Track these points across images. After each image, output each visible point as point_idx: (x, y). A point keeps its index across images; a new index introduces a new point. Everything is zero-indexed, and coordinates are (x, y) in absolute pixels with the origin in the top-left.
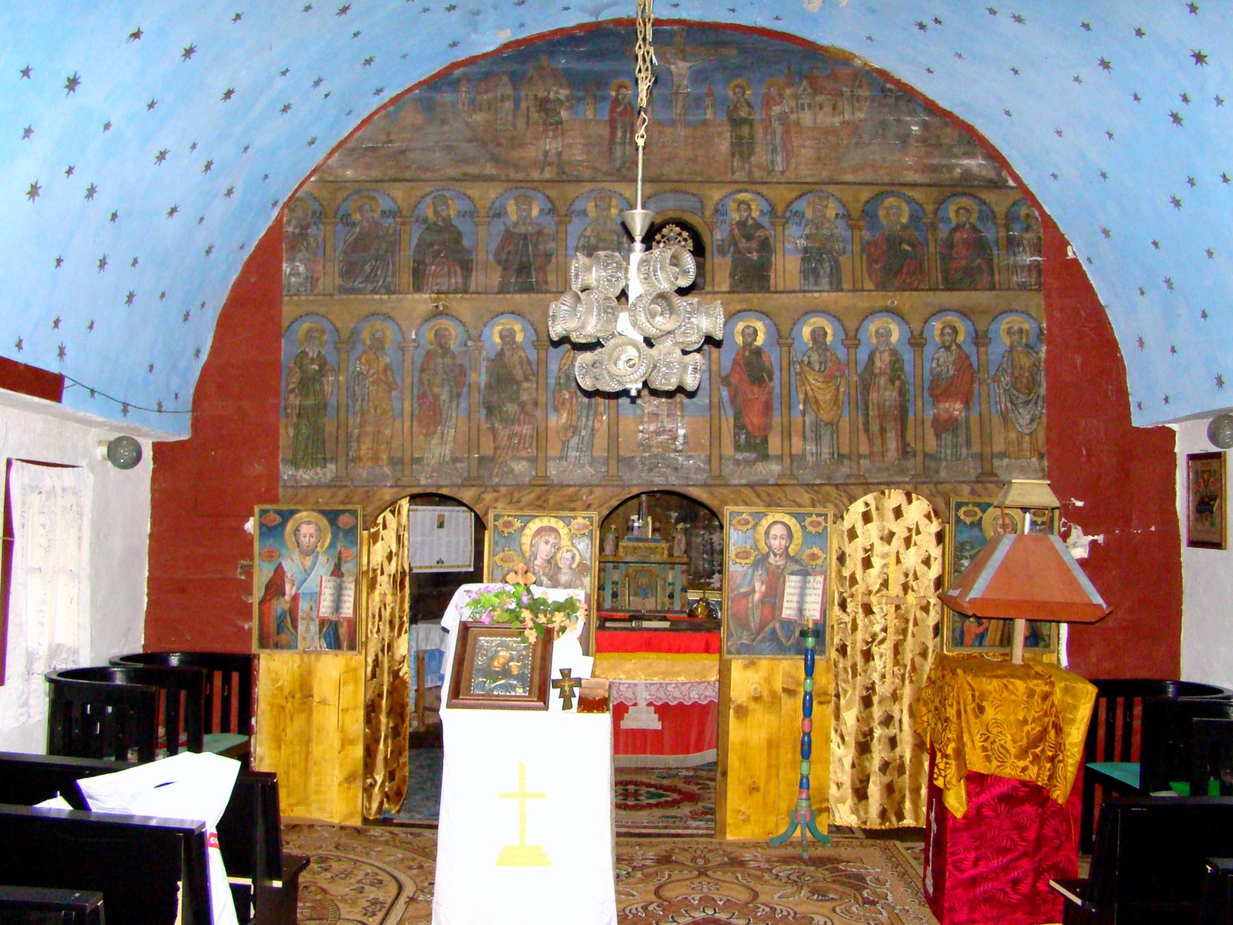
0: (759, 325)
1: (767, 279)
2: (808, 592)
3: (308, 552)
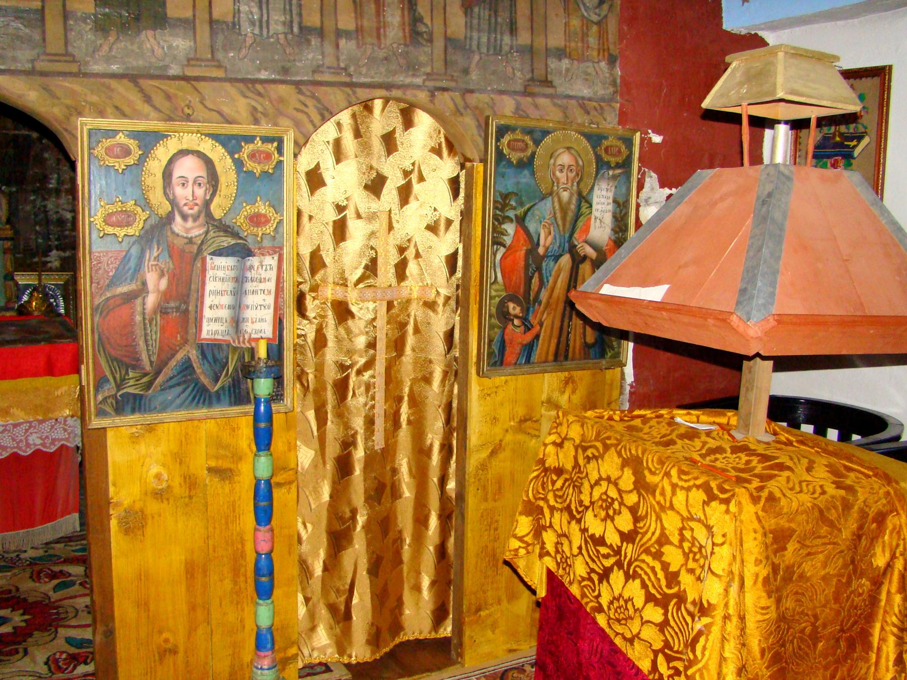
2: (249, 286)
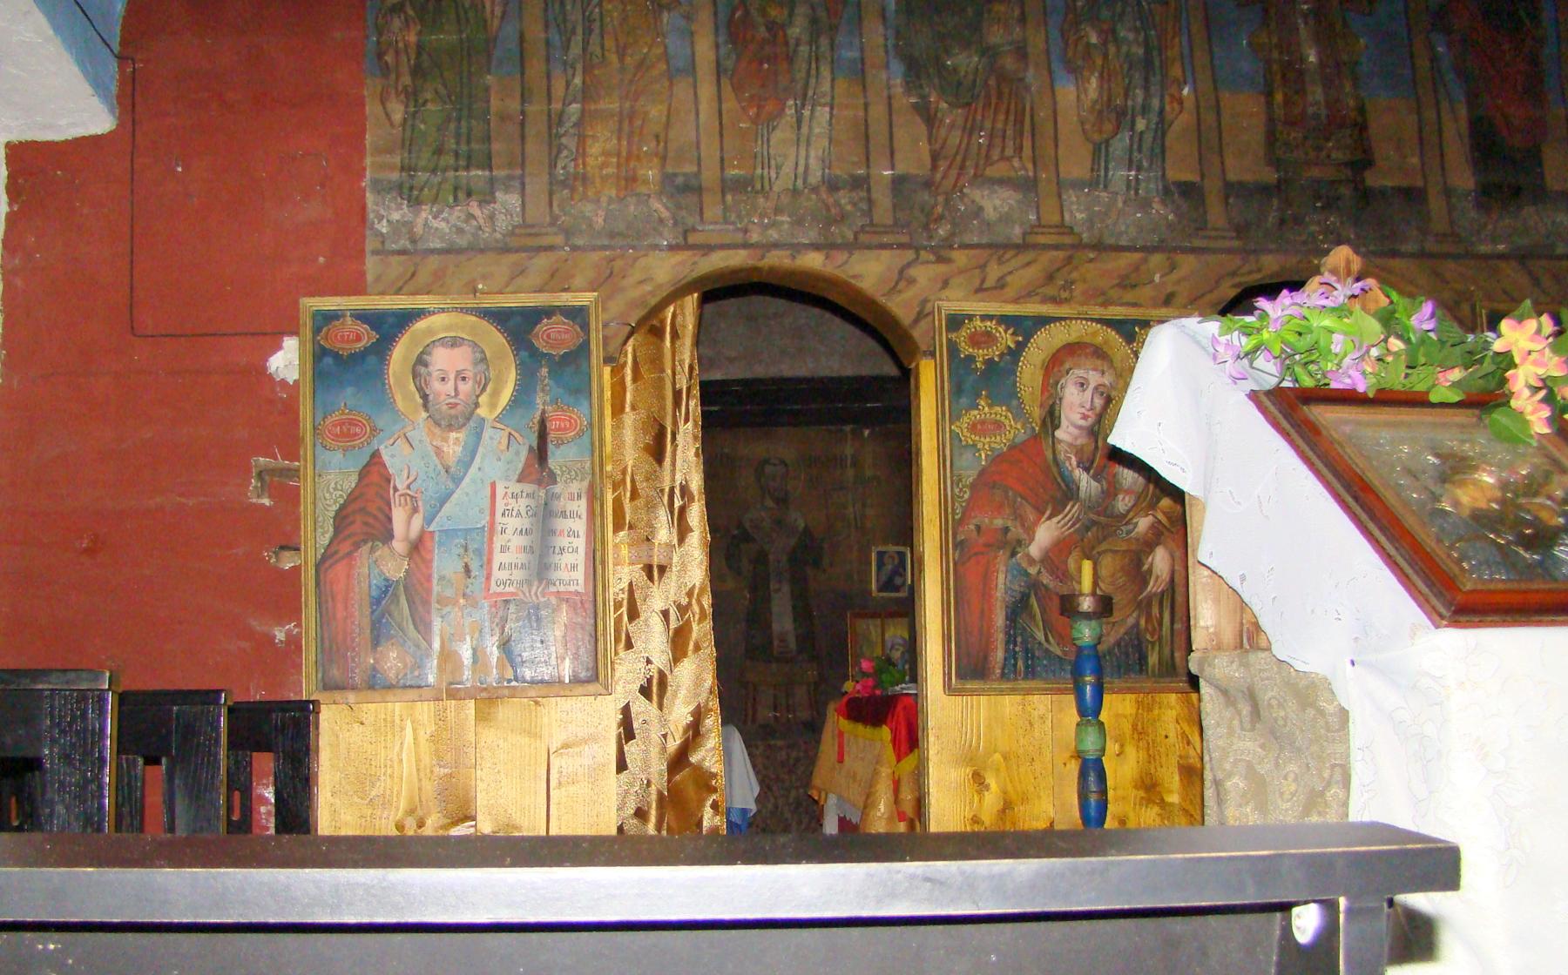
3: (462, 418)
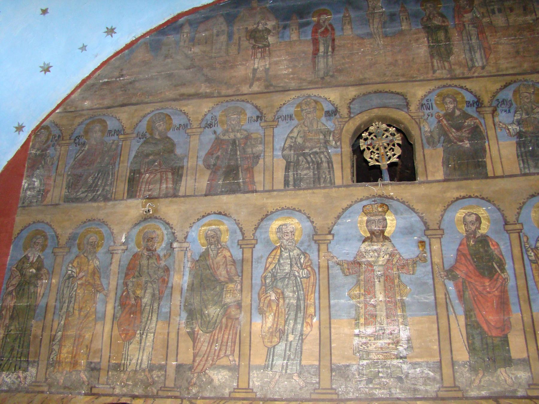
0: (482, 212)
1: (484, 166)
